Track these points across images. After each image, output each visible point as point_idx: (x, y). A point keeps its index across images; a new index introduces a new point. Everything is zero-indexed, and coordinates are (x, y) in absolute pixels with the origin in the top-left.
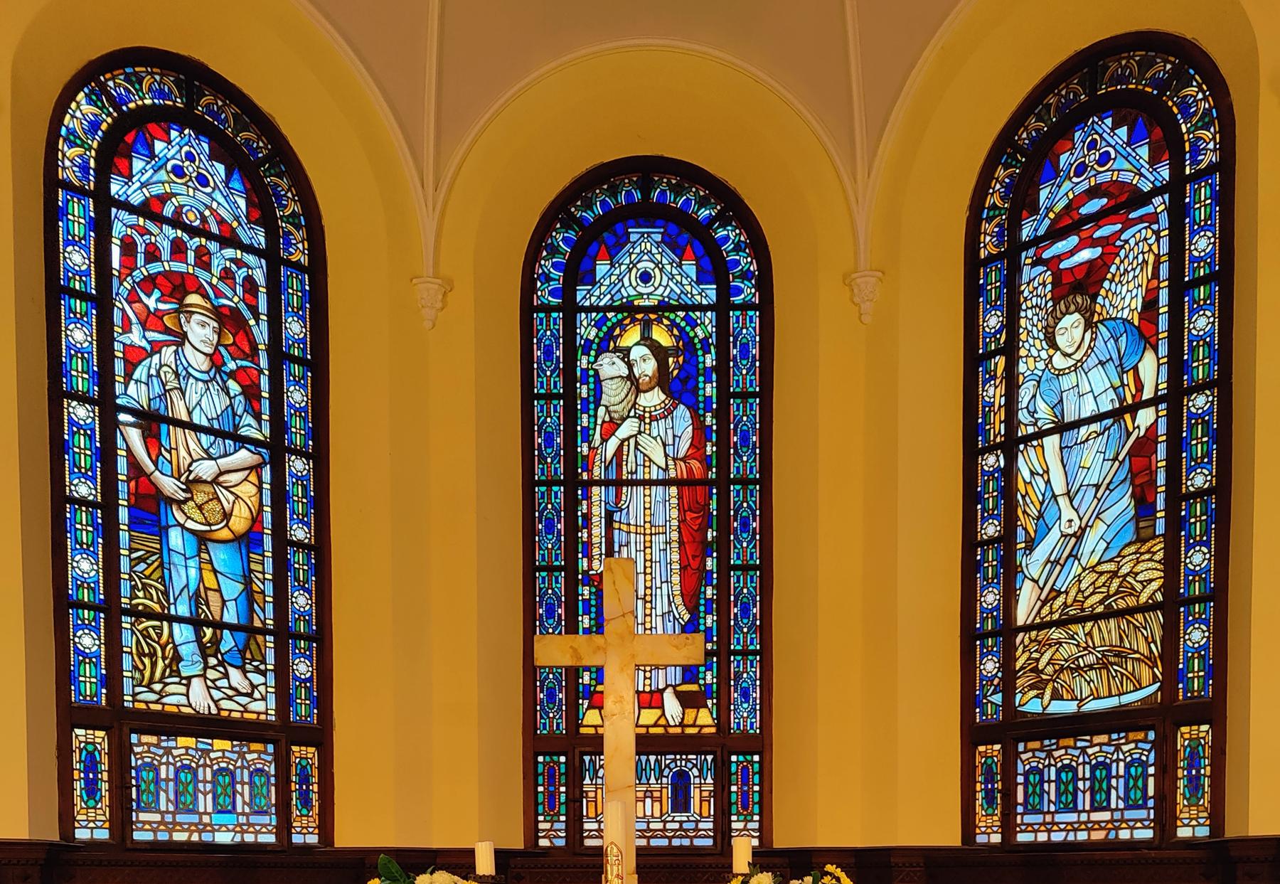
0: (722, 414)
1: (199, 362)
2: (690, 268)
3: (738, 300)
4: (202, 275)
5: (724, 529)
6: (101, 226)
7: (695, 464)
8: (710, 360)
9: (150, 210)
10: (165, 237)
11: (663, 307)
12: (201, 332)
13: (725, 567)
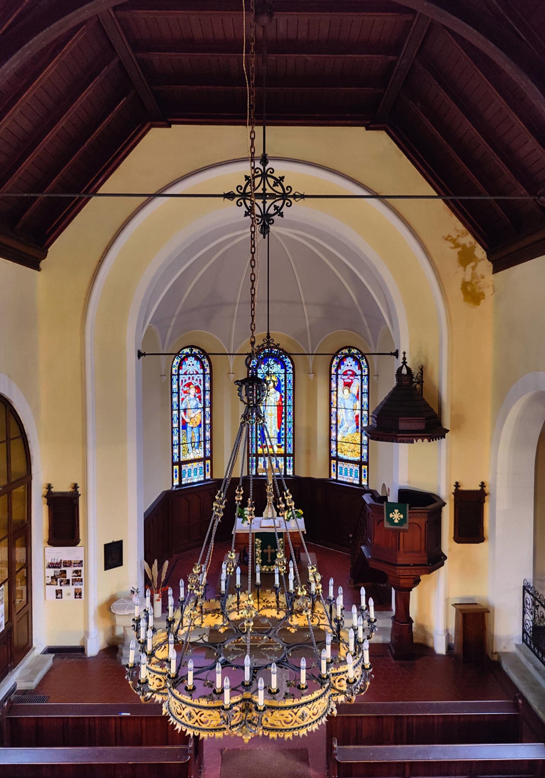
0: (285, 393)
1: (192, 396)
2: (279, 366)
3: (288, 372)
4: (193, 382)
5: (286, 414)
6: (178, 380)
7: (280, 402)
8: (283, 383)
9: (185, 374)
10: (187, 377)
11: (274, 373)
12: (193, 391)
13: (286, 422)
